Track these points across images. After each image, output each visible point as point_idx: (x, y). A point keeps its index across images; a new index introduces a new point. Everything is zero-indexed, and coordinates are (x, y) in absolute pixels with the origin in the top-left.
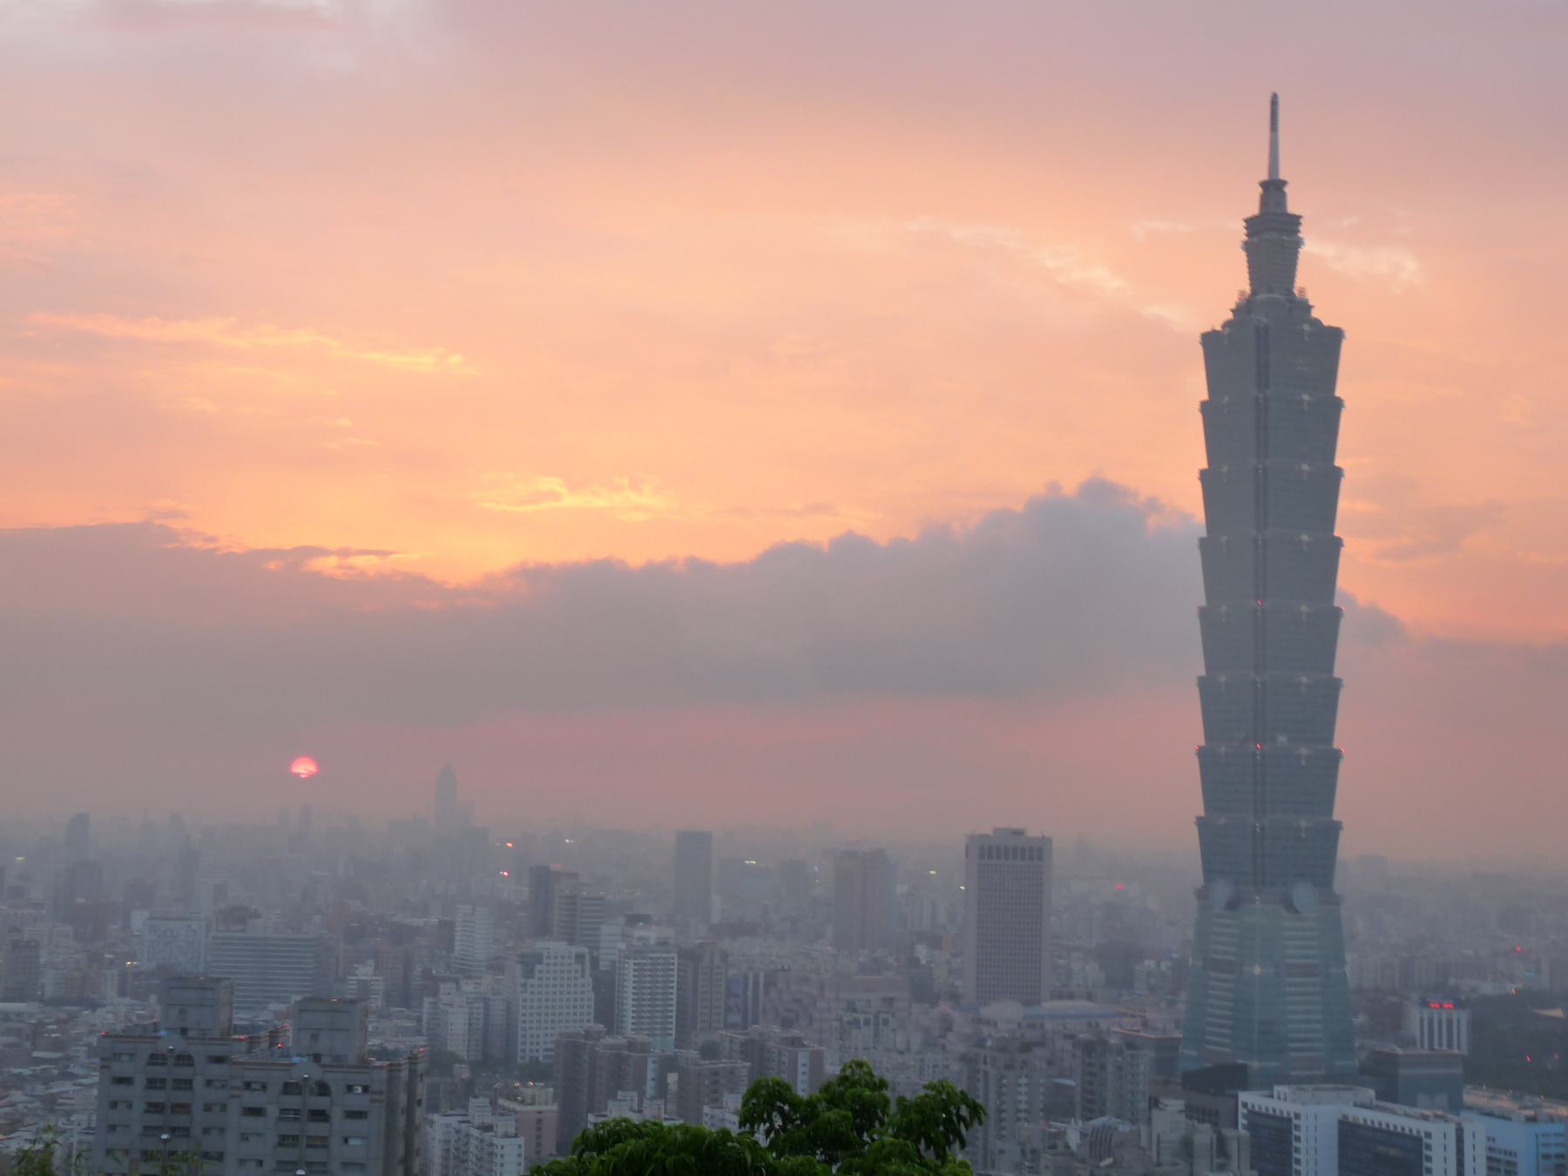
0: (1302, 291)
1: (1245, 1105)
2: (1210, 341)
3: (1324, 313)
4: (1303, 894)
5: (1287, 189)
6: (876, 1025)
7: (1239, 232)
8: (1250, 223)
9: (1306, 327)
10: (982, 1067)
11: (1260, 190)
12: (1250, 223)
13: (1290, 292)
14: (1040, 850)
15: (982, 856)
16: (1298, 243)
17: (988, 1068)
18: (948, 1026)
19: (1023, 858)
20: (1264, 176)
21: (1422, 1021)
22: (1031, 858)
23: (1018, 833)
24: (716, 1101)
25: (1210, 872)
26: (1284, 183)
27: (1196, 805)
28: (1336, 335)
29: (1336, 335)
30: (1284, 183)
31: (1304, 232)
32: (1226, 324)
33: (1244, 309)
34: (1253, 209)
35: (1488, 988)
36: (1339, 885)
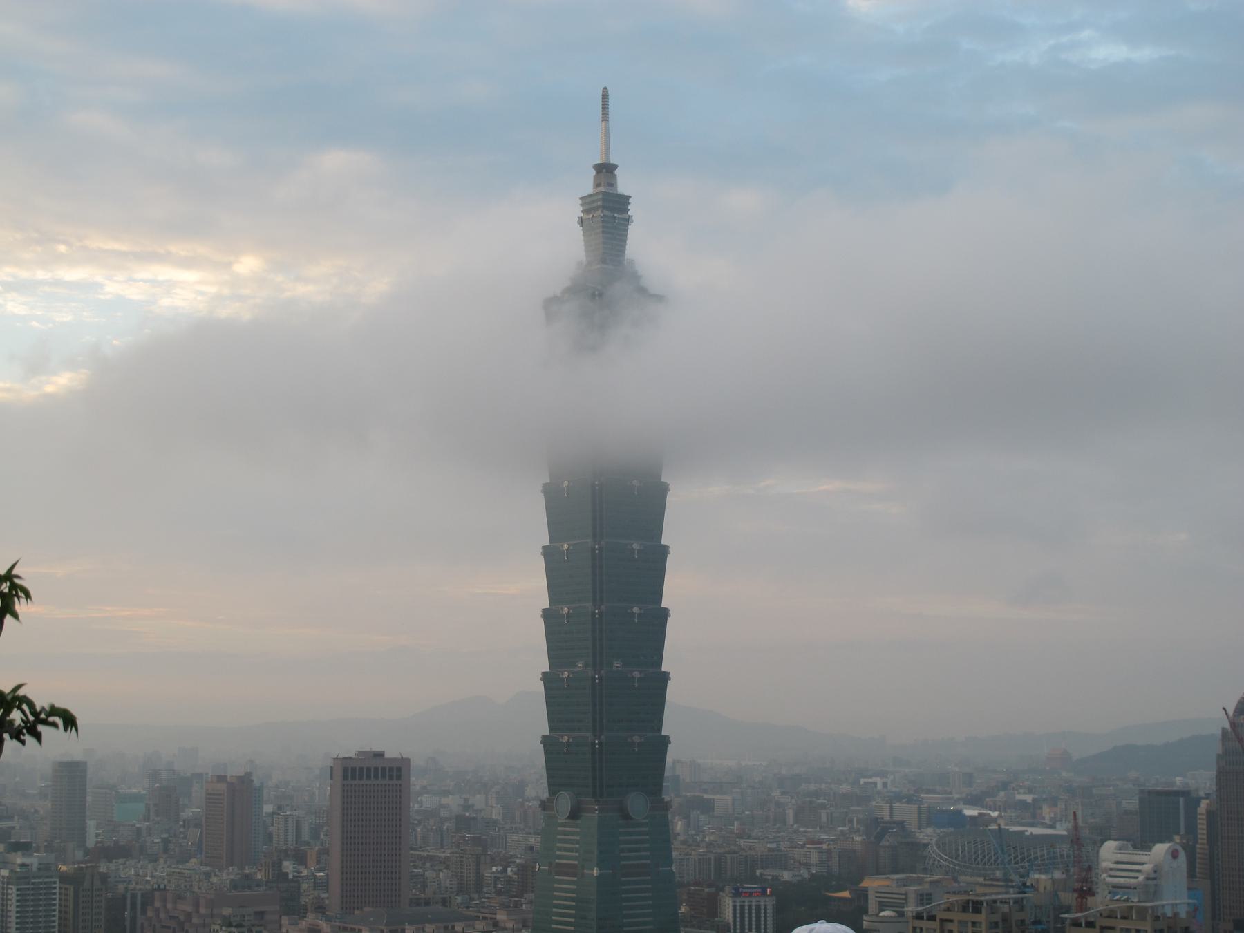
4: (636, 803)
5: (616, 172)
7: (577, 211)
11: (594, 172)
14: (399, 769)
15: (345, 778)
16: (628, 221)
20: (599, 161)
21: (735, 907)
23: (380, 755)
26: (615, 167)
27: (542, 727)
30: (615, 167)
31: (633, 210)
34: (588, 188)
35: (786, 876)
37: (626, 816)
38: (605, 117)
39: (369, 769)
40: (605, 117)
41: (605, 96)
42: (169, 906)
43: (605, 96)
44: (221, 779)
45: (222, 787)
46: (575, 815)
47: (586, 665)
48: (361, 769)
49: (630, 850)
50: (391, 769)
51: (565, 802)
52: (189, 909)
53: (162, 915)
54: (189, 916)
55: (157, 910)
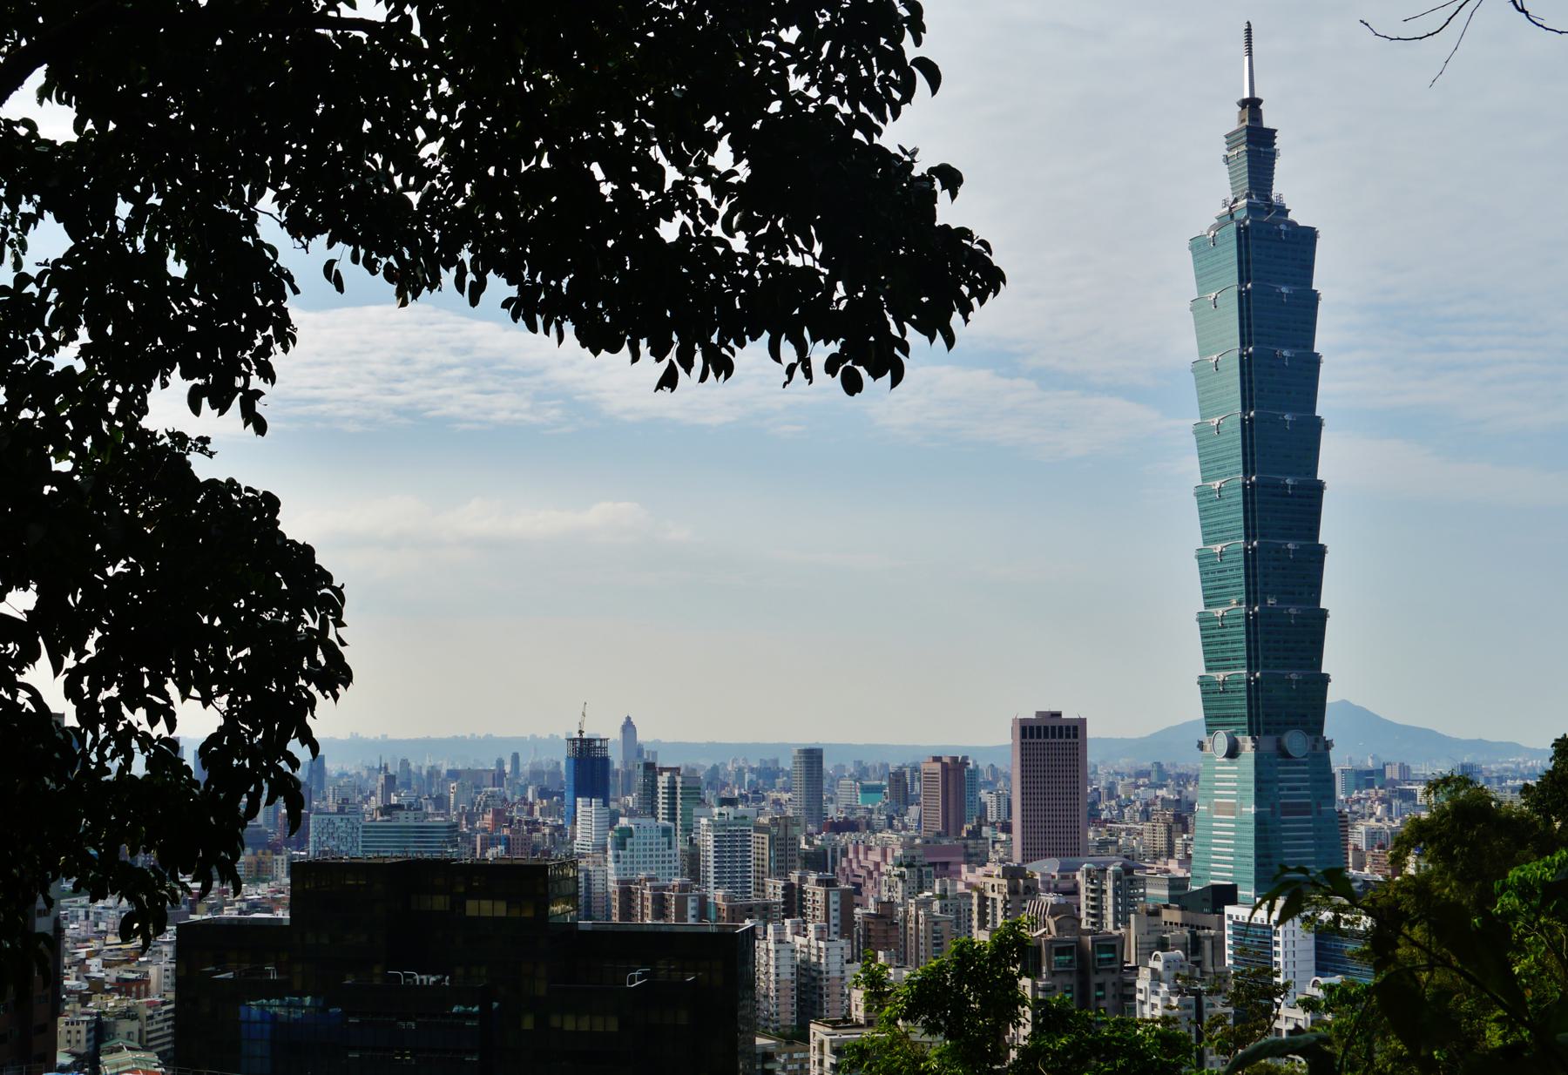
0: (1280, 196)
1: (1230, 917)
2: (1197, 245)
3: (1300, 216)
4: (1295, 742)
6: (920, 877)
7: (1222, 149)
9: (1282, 227)
10: (990, 894)
13: (1268, 198)
14: (1075, 728)
15: (1023, 735)
17: (995, 895)
19: (1061, 736)
22: (1068, 736)
23: (1058, 715)
25: (1211, 727)
26: (1260, 101)
30: (1260, 101)
31: (1279, 143)
36: (1328, 733)
37: (1284, 753)
38: (1250, 54)
39: (1046, 728)
40: (1250, 54)
41: (1249, 31)
42: (861, 857)
43: (1249, 31)
44: (937, 759)
45: (937, 767)
46: (1233, 752)
47: (1239, 603)
48: (1039, 728)
49: (1290, 789)
50: (1068, 728)
51: (1221, 741)
52: (878, 859)
53: (855, 866)
54: (877, 865)
55: (850, 861)
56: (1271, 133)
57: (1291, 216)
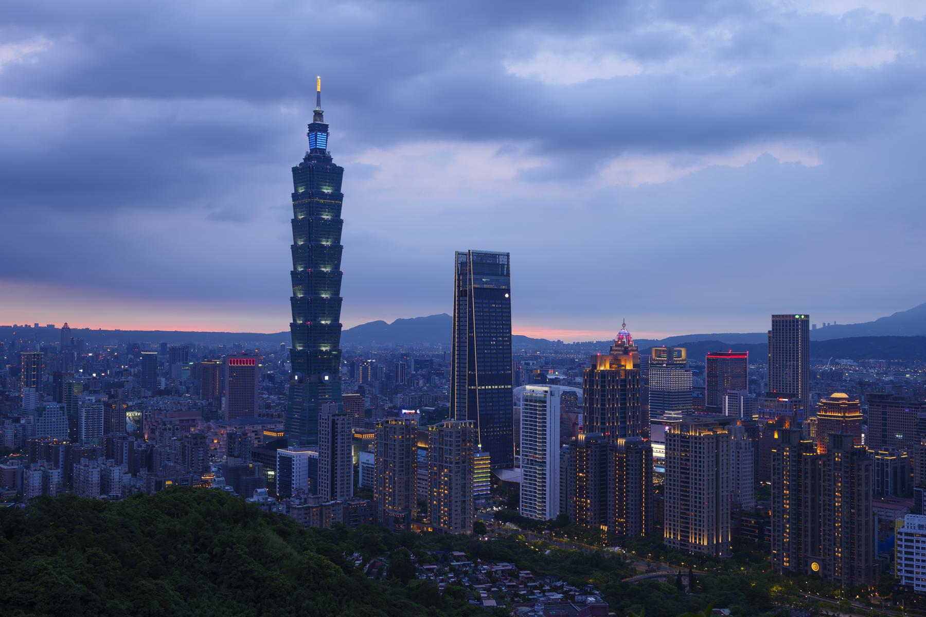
2: (295, 170)
7: (307, 130)
8: (310, 126)
12: (310, 126)
18: (209, 428)
24: (79, 462)
28: (341, 170)
29: (341, 170)
32: (301, 164)
33: (308, 158)
34: (311, 122)
56: (326, 126)
57: (333, 162)
